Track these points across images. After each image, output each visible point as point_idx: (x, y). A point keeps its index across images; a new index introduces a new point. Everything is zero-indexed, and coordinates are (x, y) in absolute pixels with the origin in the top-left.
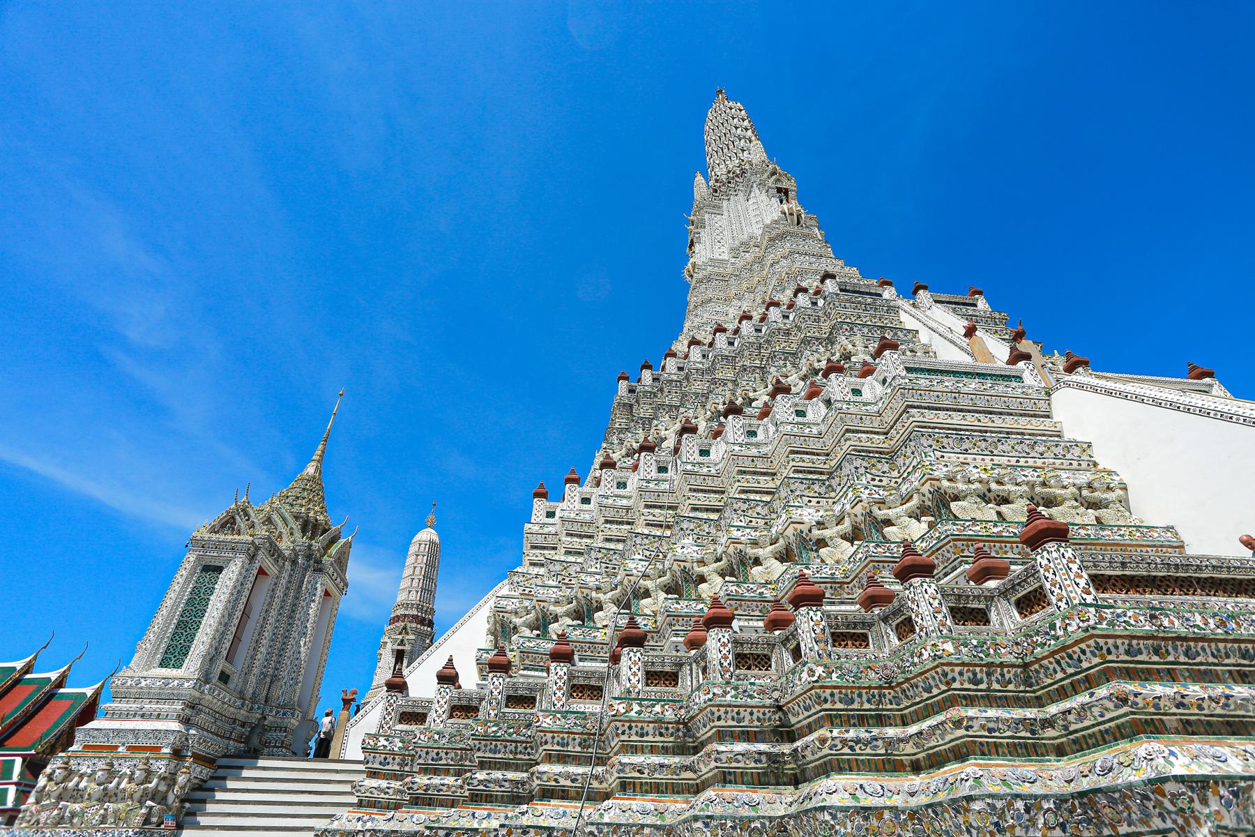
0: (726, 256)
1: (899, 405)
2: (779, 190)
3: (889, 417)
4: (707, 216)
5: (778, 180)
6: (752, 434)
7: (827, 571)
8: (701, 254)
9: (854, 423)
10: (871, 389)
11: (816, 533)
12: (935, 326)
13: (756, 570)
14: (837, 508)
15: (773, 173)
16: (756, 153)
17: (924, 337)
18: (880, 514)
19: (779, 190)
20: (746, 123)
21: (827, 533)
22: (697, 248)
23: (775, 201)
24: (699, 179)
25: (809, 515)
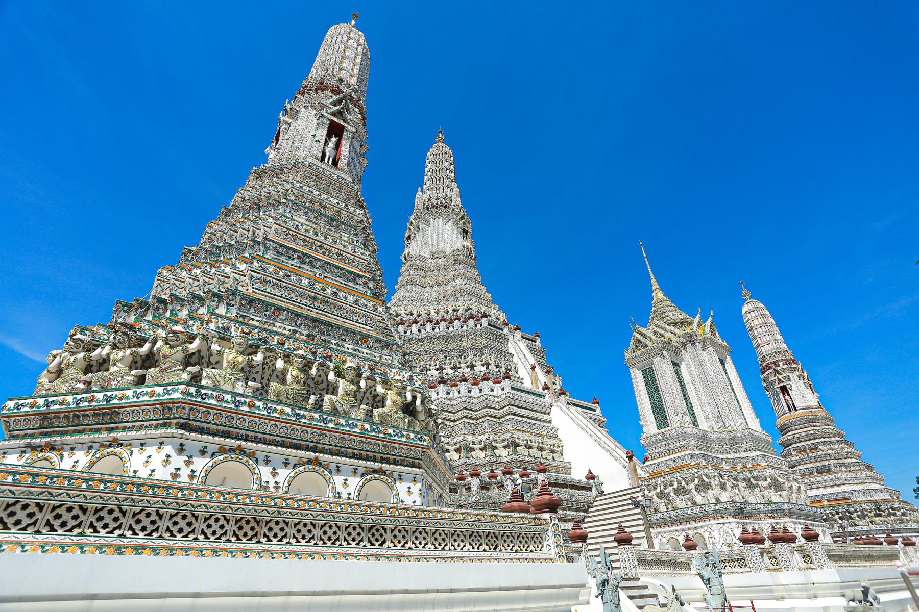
0: (427, 255)
1: (506, 403)
2: (464, 230)
3: (502, 405)
4: (421, 225)
5: (464, 223)
6: (448, 393)
7: (474, 461)
8: (414, 249)
9: (490, 404)
10: (497, 391)
11: (471, 445)
12: (520, 352)
13: (447, 454)
14: (480, 438)
15: (463, 218)
16: (455, 195)
17: (515, 359)
18: (494, 444)
19: (464, 230)
20: (452, 167)
21: (475, 447)
22: (413, 243)
23: (460, 236)
24: (419, 193)
25: (470, 438)
